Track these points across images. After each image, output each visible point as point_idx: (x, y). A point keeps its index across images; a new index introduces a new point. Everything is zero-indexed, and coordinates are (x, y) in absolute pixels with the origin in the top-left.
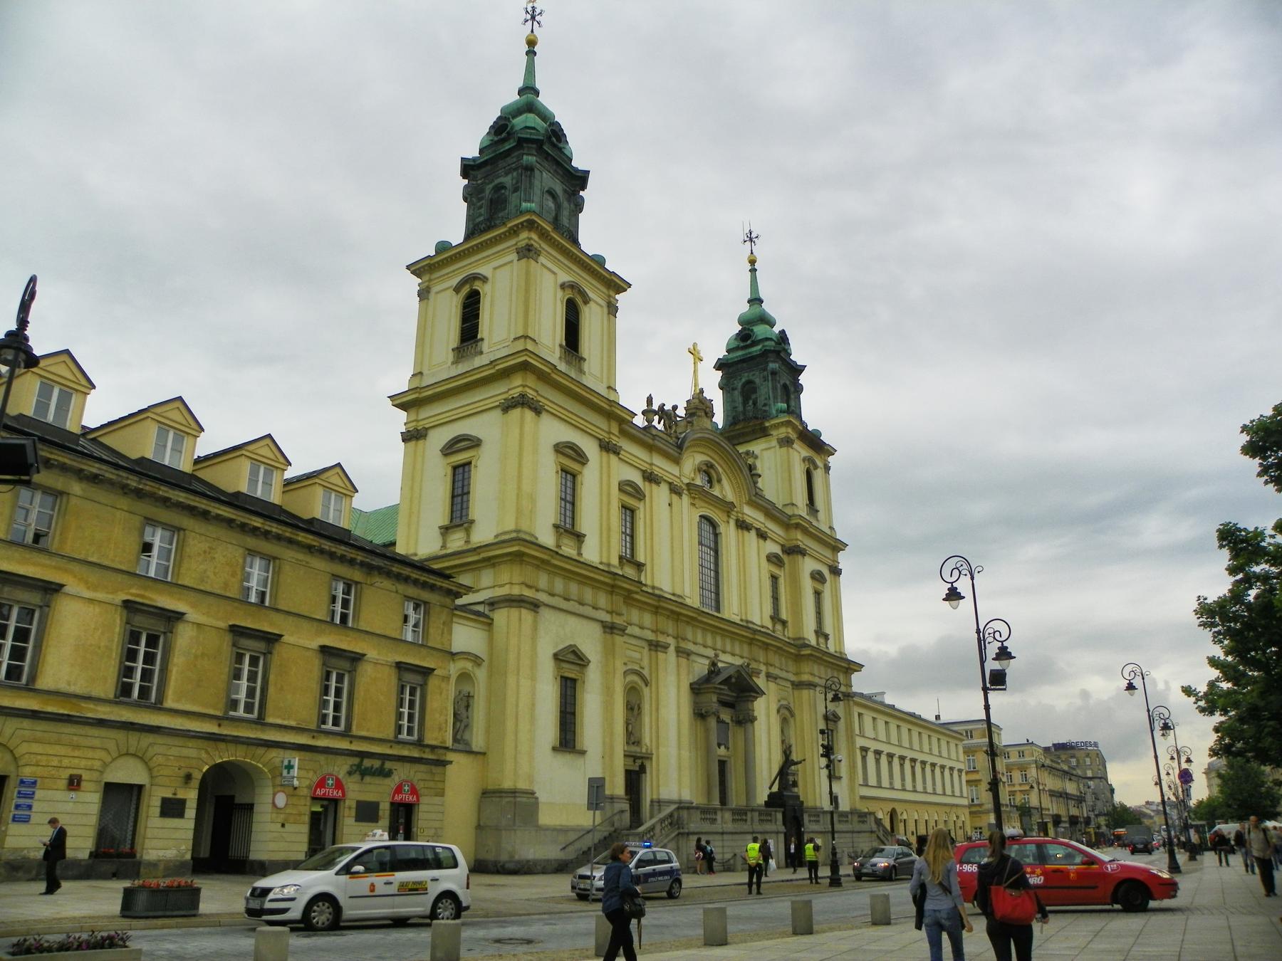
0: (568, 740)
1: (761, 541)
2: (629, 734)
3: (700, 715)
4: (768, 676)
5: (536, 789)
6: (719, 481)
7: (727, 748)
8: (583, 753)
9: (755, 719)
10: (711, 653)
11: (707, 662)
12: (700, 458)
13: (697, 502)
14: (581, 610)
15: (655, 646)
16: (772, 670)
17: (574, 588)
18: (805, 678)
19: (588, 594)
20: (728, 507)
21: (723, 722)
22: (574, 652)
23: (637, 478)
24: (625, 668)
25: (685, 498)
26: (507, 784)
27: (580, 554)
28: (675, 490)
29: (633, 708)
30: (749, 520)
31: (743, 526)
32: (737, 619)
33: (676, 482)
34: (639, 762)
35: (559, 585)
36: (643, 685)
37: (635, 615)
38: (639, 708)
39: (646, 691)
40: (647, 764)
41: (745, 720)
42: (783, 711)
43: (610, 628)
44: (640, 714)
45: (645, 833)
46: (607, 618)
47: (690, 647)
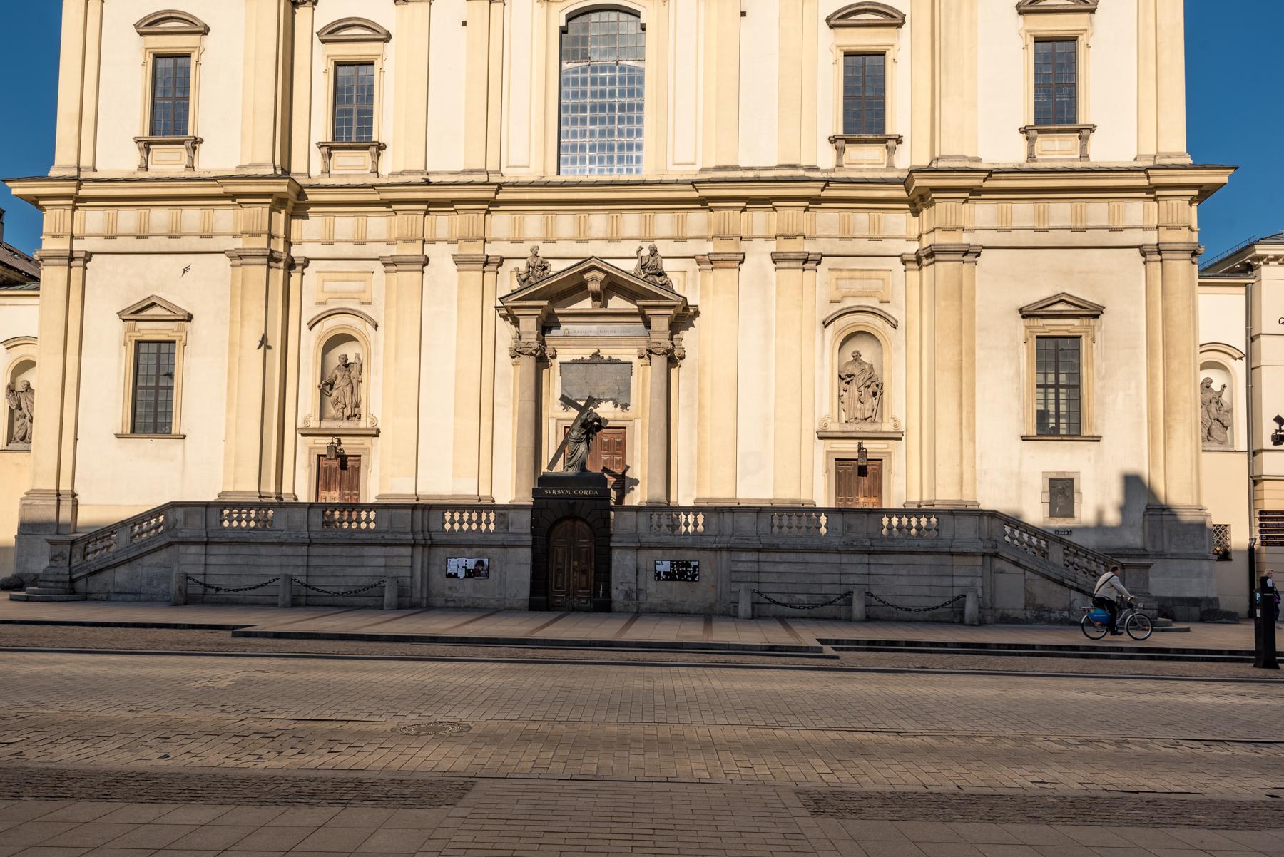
4: (777, 259)
7: (625, 406)
10: (525, 249)
11: (522, 265)
14: (175, 244)
15: (392, 263)
16: (790, 247)
17: (160, 217)
19: (192, 217)
21: (611, 361)
22: (153, 304)
24: (321, 310)
27: (191, 167)
32: (691, 173)
35: (128, 218)
36: (370, 328)
37: (345, 224)
43: (238, 257)
46: (239, 244)
47: (493, 250)
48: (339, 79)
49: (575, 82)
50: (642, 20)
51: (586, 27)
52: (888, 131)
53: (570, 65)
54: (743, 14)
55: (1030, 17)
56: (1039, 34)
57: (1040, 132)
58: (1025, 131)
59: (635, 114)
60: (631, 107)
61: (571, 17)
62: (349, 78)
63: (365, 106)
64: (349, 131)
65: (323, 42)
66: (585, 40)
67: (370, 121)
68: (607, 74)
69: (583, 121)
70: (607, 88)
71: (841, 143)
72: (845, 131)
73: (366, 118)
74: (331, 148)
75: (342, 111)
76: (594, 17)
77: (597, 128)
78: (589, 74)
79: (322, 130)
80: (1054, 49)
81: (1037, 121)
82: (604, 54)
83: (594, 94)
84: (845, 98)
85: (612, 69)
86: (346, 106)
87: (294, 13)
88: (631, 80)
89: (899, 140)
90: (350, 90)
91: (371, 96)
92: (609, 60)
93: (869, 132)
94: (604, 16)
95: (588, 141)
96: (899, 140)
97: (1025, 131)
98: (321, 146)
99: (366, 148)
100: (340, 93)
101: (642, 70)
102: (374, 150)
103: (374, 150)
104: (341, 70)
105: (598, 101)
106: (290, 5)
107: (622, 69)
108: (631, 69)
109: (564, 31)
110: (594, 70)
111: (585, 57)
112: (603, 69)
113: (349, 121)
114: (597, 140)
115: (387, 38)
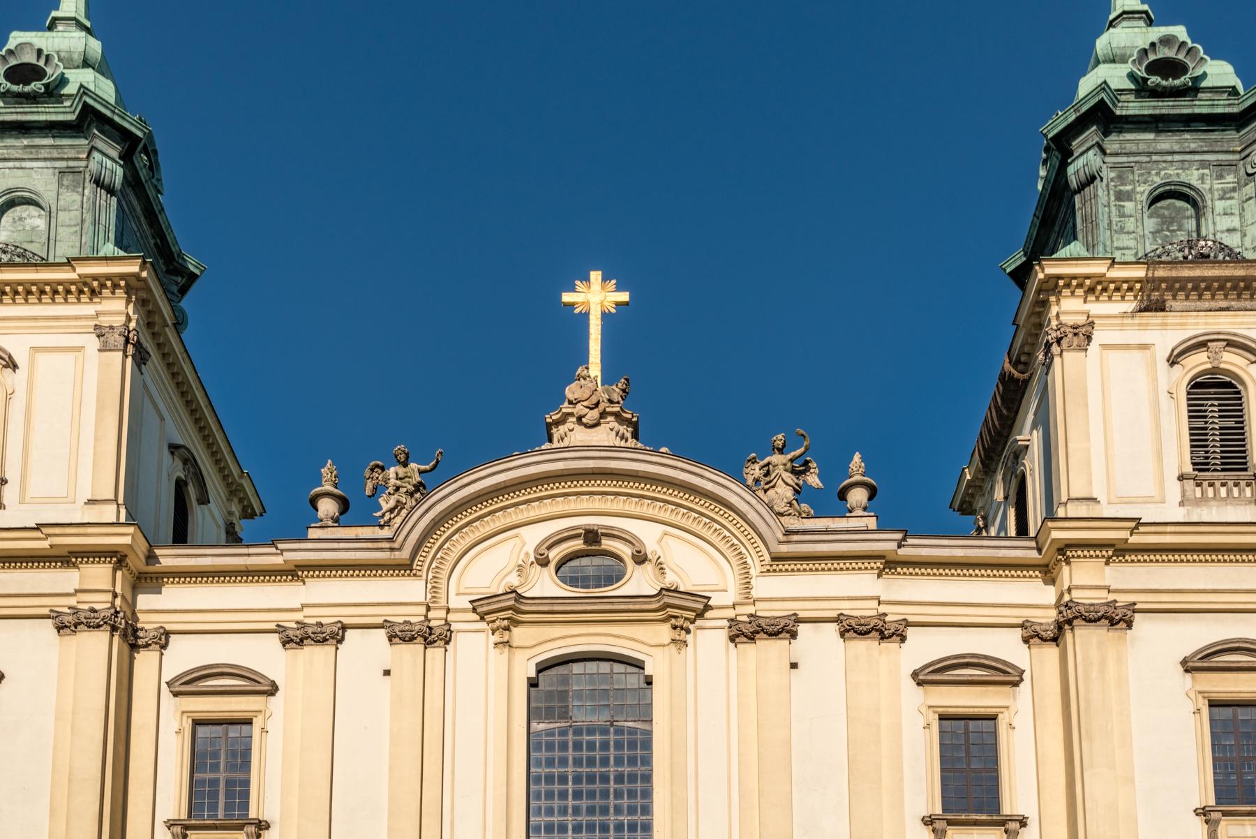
1: (866, 647)
6: (640, 559)
12: (534, 536)
13: (520, 634)
20: (681, 610)
23: (263, 655)
25: (472, 643)
28: (400, 635)
30: (764, 610)
31: (747, 632)
33: (415, 616)
48: (198, 741)
49: (550, 746)
50: (648, 671)
51: (565, 680)
52: (1007, 810)
53: (542, 726)
54: (794, 666)
55: (1199, 675)
56: (1215, 696)
57: (1225, 814)
58: (1203, 812)
59: (639, 786)
60: (633, 778)
61: (542, 668)
62: (213, 741)
63: (239, 775)
64: (213, 807)
65: (176, 694)
66: (563, 695)
67: (246, 794)
68: (597, 738)
69: (563, 795)
70: (584, 786)
71: (940, 825)
72: (944, 810)
73: (240, 791)
74: (187, 827)
75: (202, 782)
76: (577, 668)
77: (584, 803)
78: (570, 737)
79: (173, 803)
80: (1235, 716)
81: (1219, 800)
82: (594, 709)
83: (578, 762)
84: (942, 770)
85: (605, 731)
86: (209, 776)
87: (132, 659)
88: (632, 745)
89: (1023, 822)
90: (215, 755)
91: (246, 764)
92: (601, 719)
93: (979, 810)
94: (591, 667)
95: (570, 819)
96: (1023, 822)
97: (1203, 812)
98: (170, 824)
99: (240, 828)
100: (199, 759)
101: (650, 733)
102: (252, 829)
103: (251, 829)
104: (202, 731)
105: (585, 770)
106: (126, 648)
107: (619, 731)
108: (632, 731)
109: (533, 684)
110: (578, 732)
111: (564, 715)
112: (591, 731)
113: (214, 795)
114: (584, 819)
115: (273, 690)
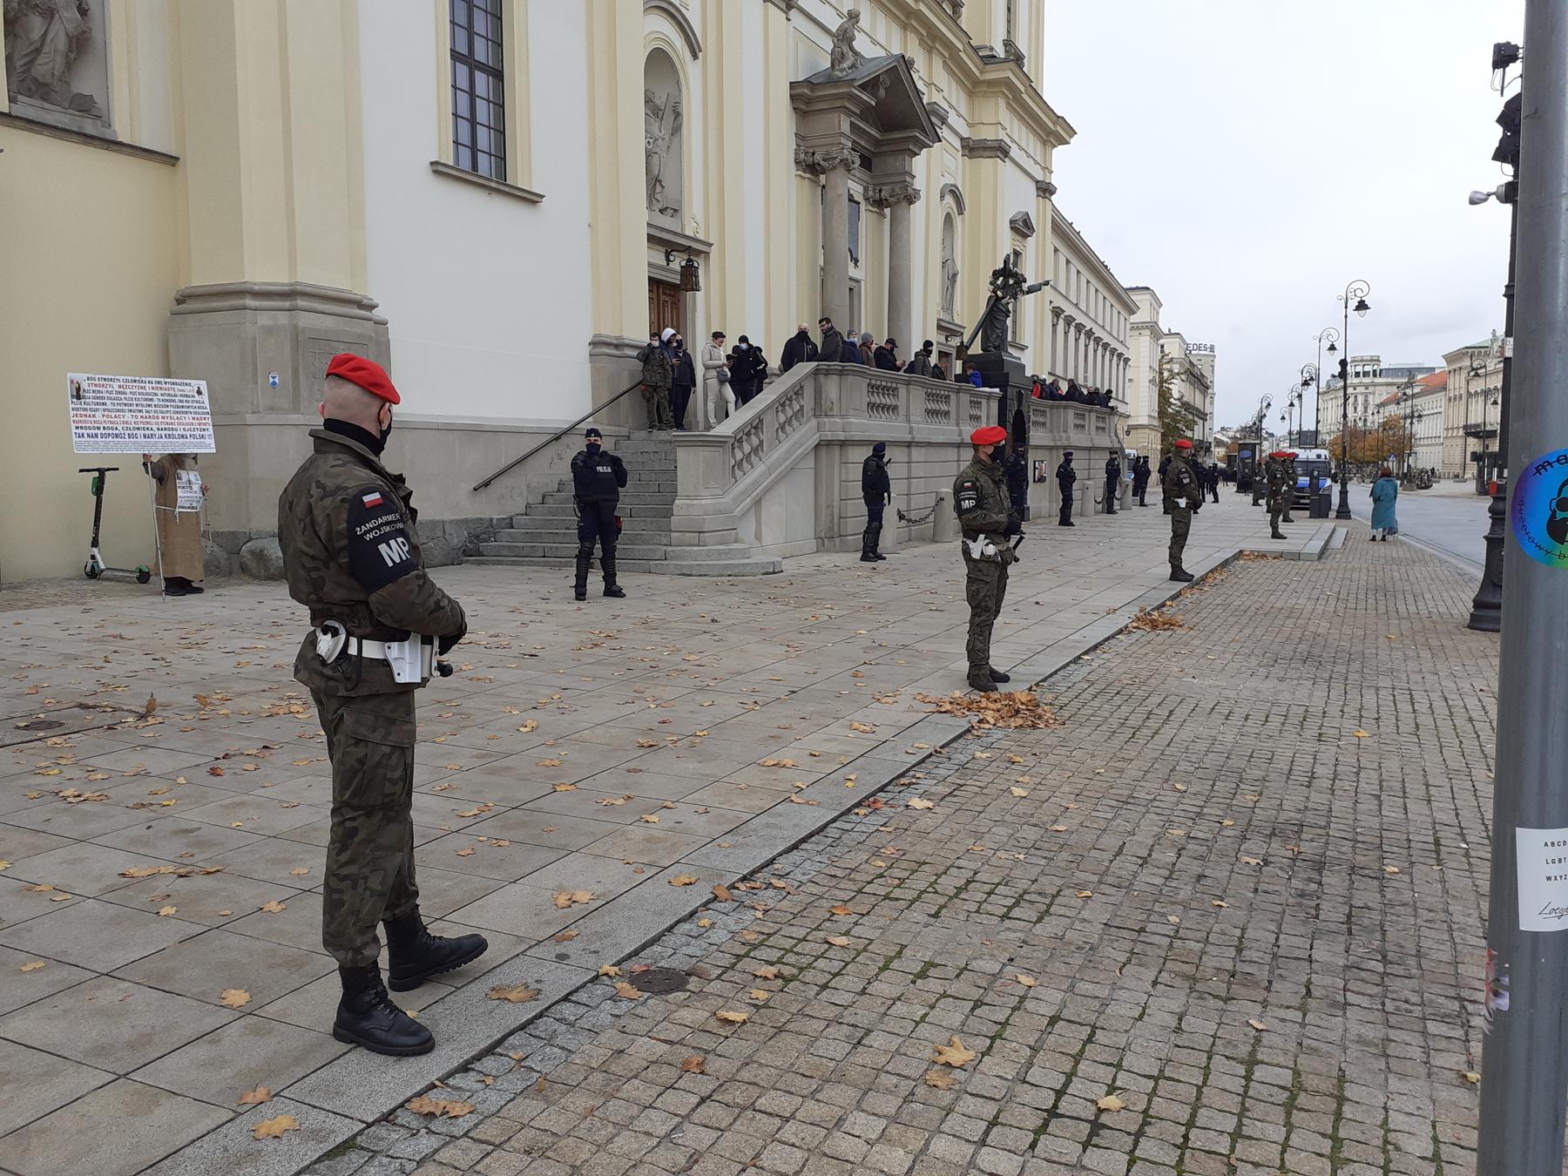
0: (483, 154)
2: (654, 183)
3: (811, 167)
5: (372, 293)
8: (530, 199)
9: (911, 199)
18: (987, 134)
26: (263, 272)
29: (664, 112)
34: (678, 262)
38: (678, 115)
39: (692, 72)
40: (699, 262)
41: (892, 197)
42: (949, 199)
44: (677, 130)
45: (738, 440)
